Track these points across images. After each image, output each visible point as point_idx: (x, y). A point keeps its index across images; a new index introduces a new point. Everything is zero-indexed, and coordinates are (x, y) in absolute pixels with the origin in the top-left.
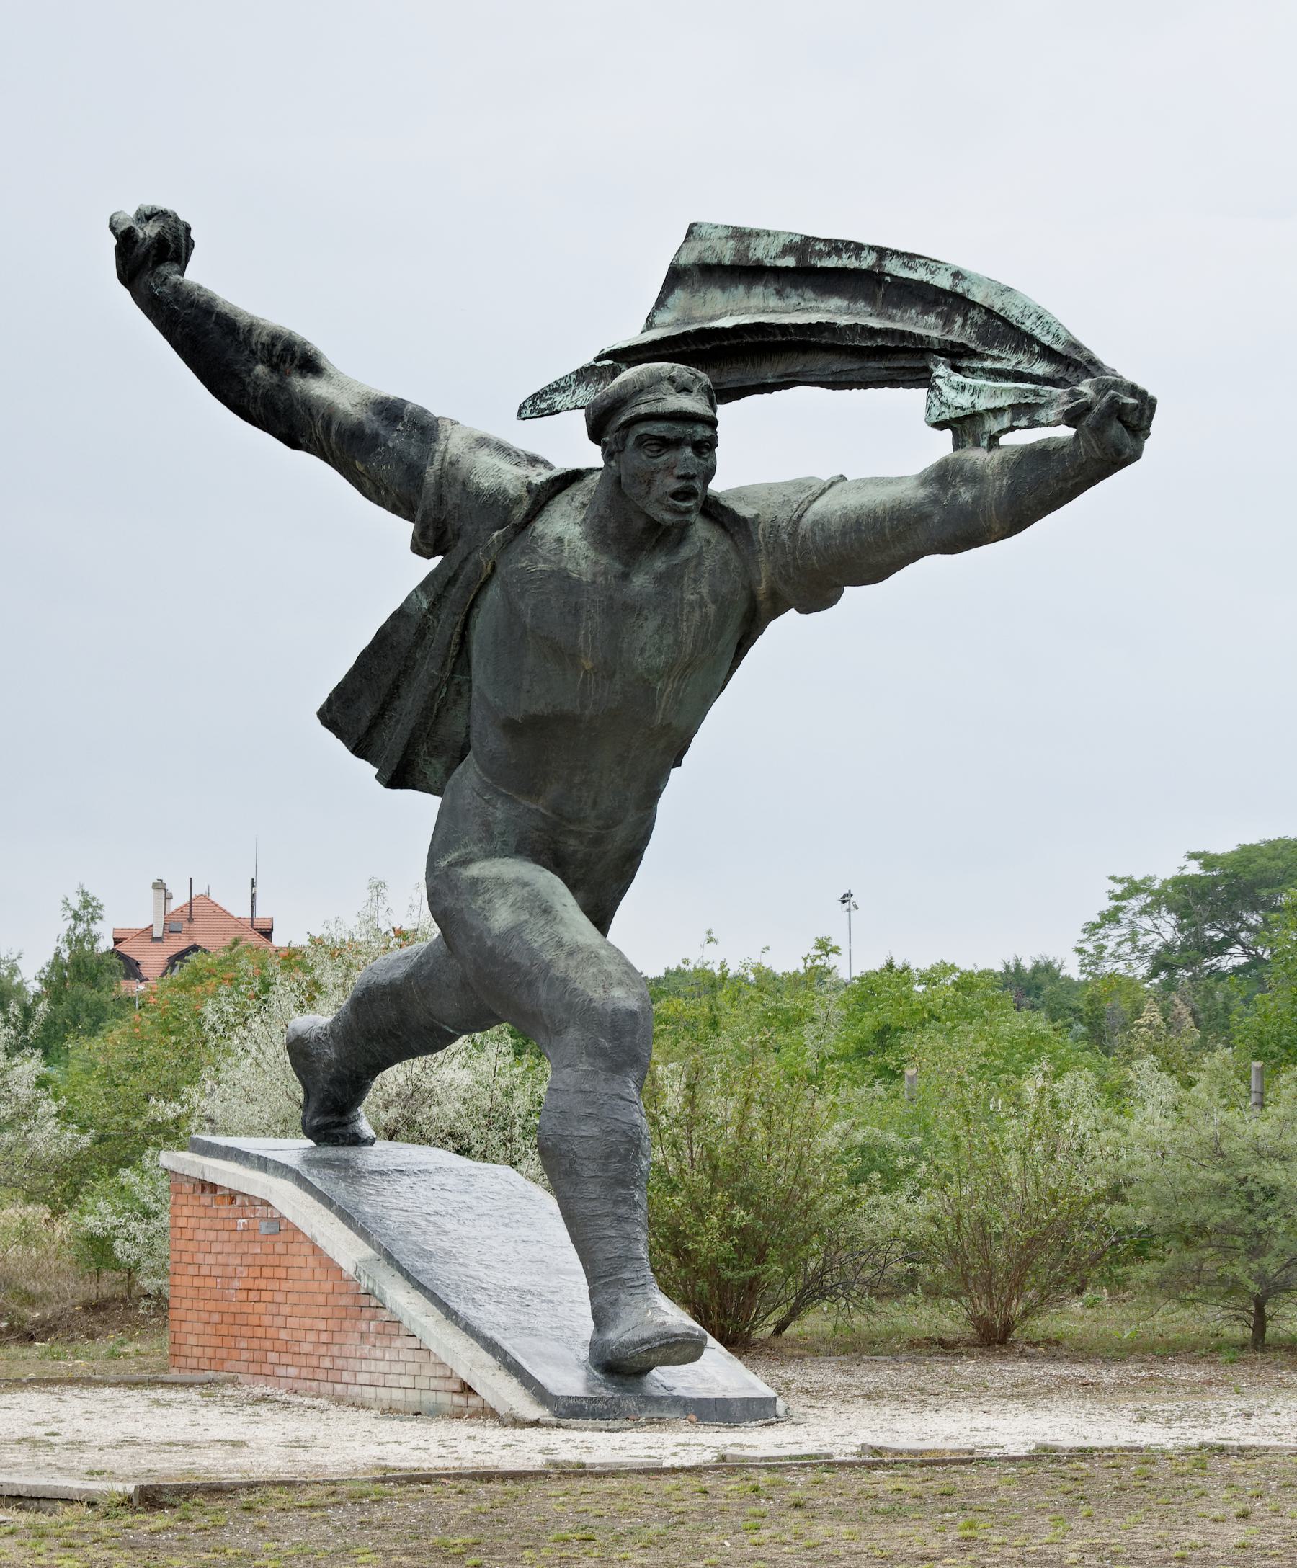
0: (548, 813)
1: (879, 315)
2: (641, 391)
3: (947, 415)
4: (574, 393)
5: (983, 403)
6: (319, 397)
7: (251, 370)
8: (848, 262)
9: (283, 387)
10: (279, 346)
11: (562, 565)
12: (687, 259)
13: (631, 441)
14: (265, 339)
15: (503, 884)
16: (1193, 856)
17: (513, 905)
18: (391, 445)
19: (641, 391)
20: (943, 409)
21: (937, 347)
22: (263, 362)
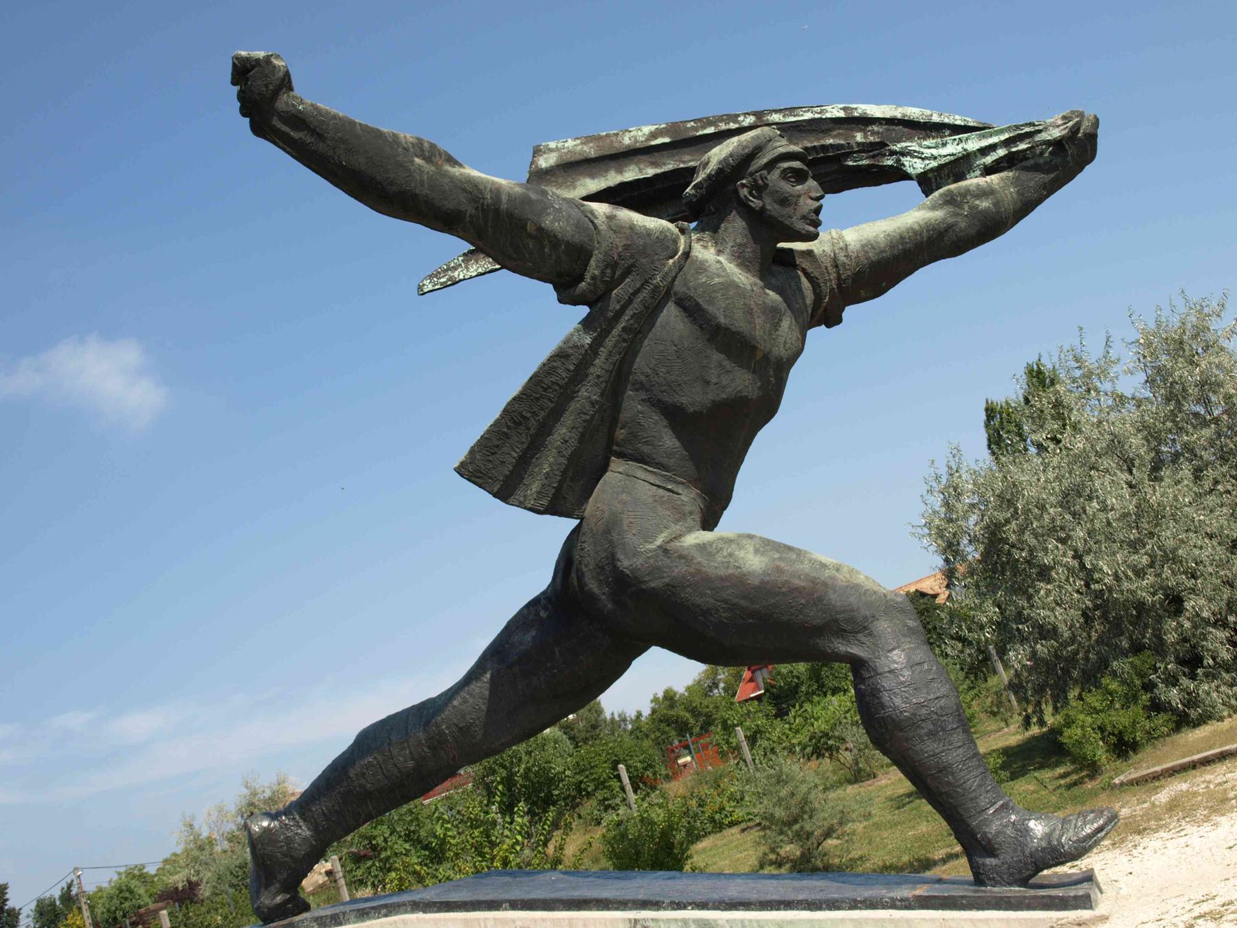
20: (927, 162)
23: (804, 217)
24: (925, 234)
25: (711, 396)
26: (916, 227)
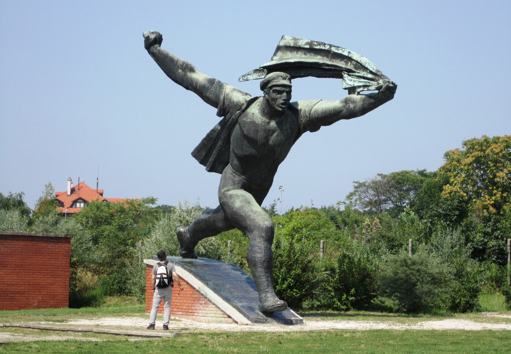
1: (330, 60)
2: (274, 79)
3: (347, 86)
4: (253, 75)
5: (356, 84)
6: (194, 78)
7: (178, 71)
8: (322, 47)
9: (185, 75)
10: (185, 65)
11: (254, 120)
12: (282, 44)
13: (271, 91)
14: (181, 63)
15: (237, 196)
16: (379, 175)
17: (241, 201)
18: (212, 90)
19: (274, 79)
20: (346, 85)
21: (344, 69)
22: (180, 69)
23: (278, 105)
24: (333, 112)
25: (243, 153)
26: (331, 109)
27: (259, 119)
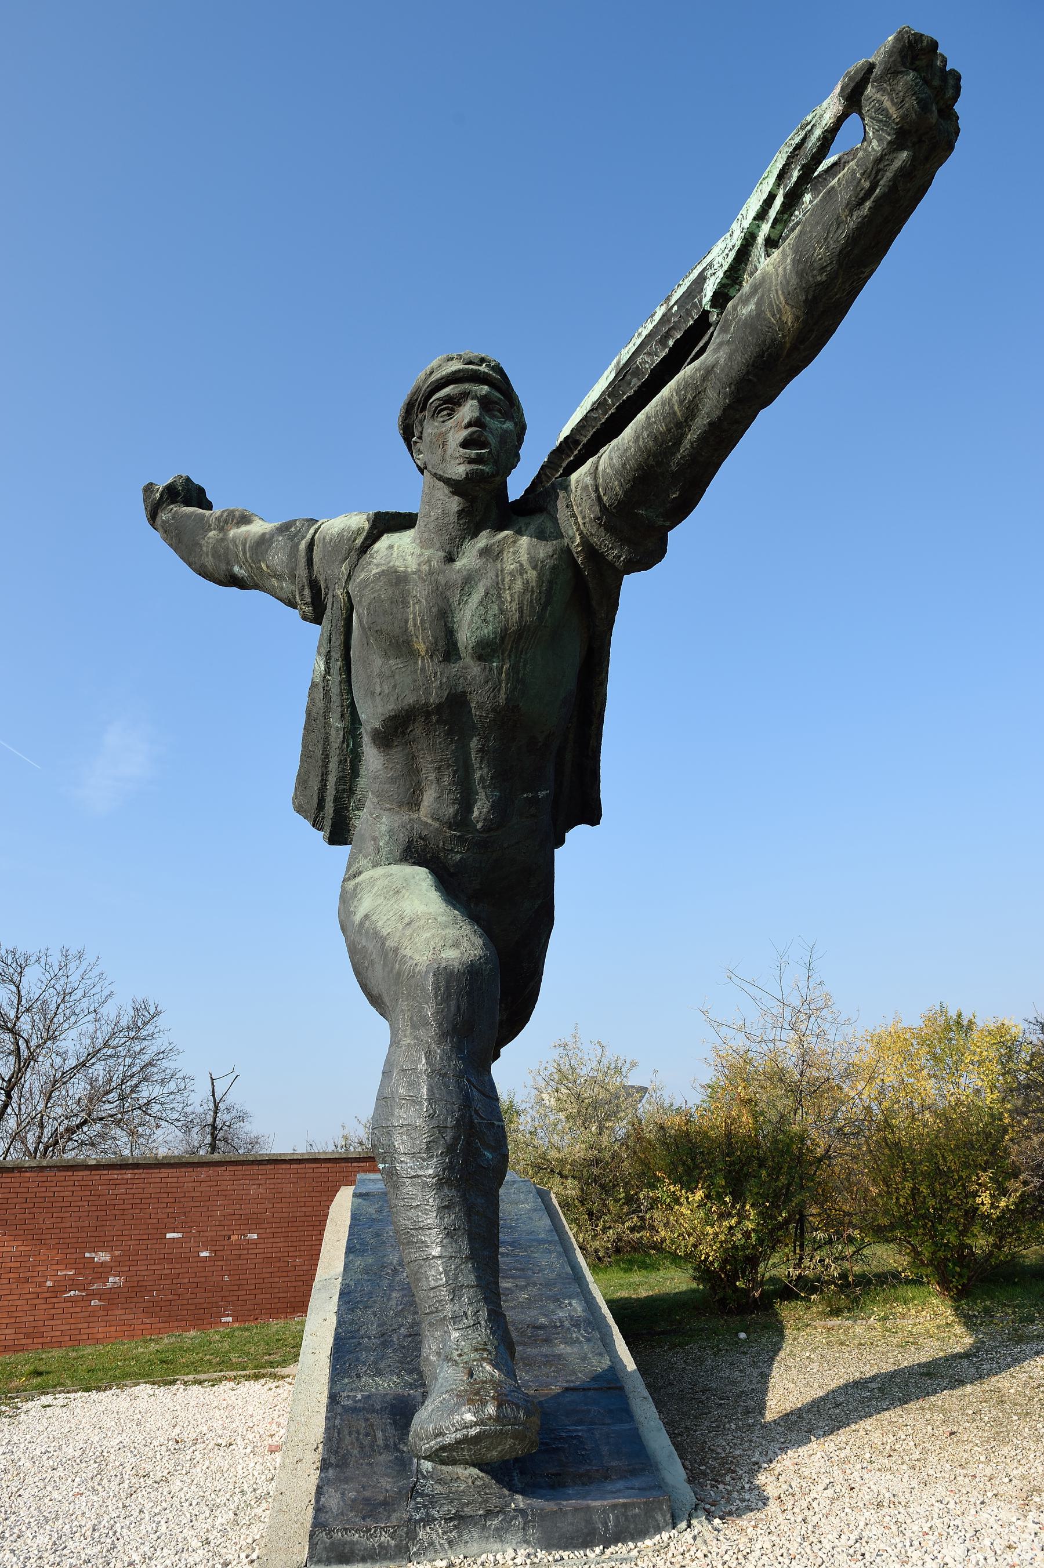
0: (429, 821)
11: (391, 564)
15: (373, 881)
22: (215, 529)
25: (380, 710)
27: (409, 558)
